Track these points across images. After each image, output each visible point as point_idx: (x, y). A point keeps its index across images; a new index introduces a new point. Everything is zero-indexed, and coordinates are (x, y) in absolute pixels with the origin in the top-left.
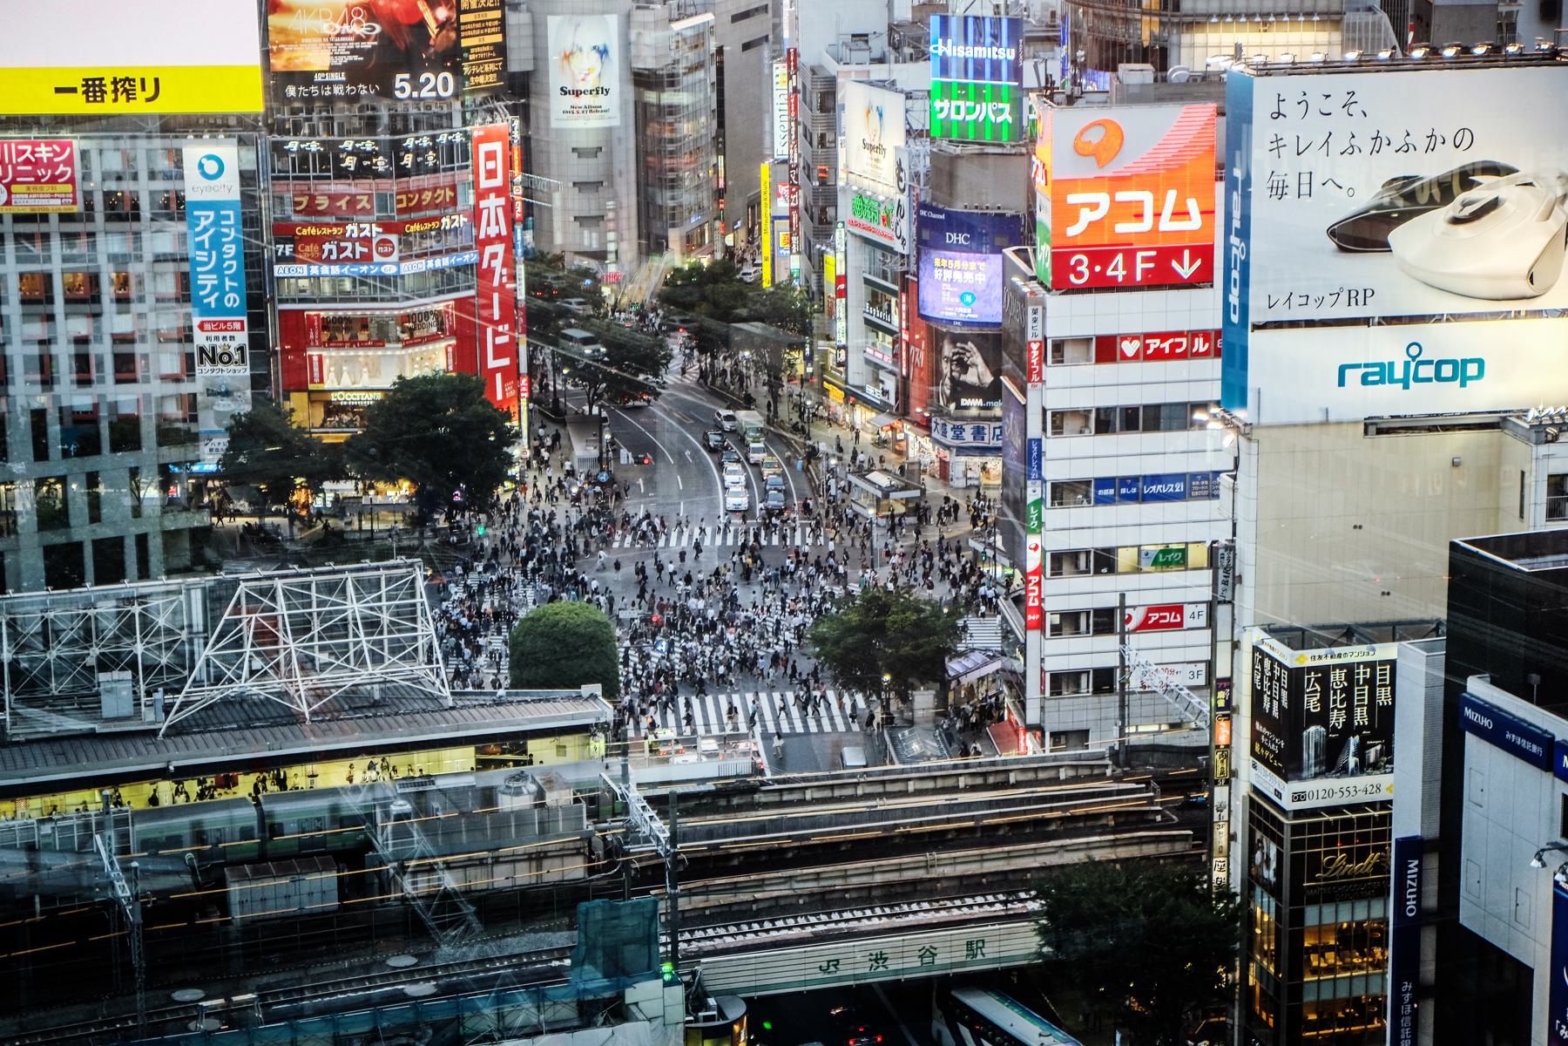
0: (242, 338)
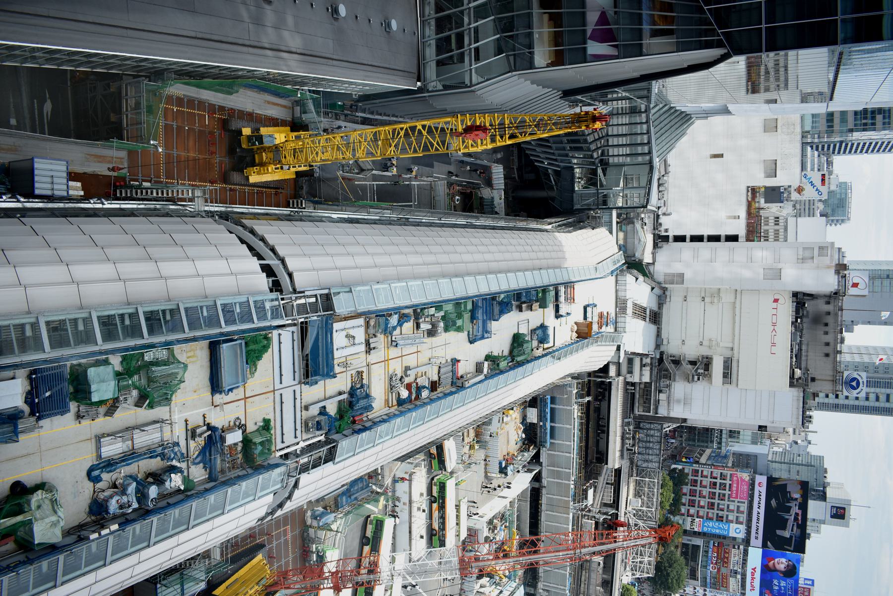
0: (696, 530)
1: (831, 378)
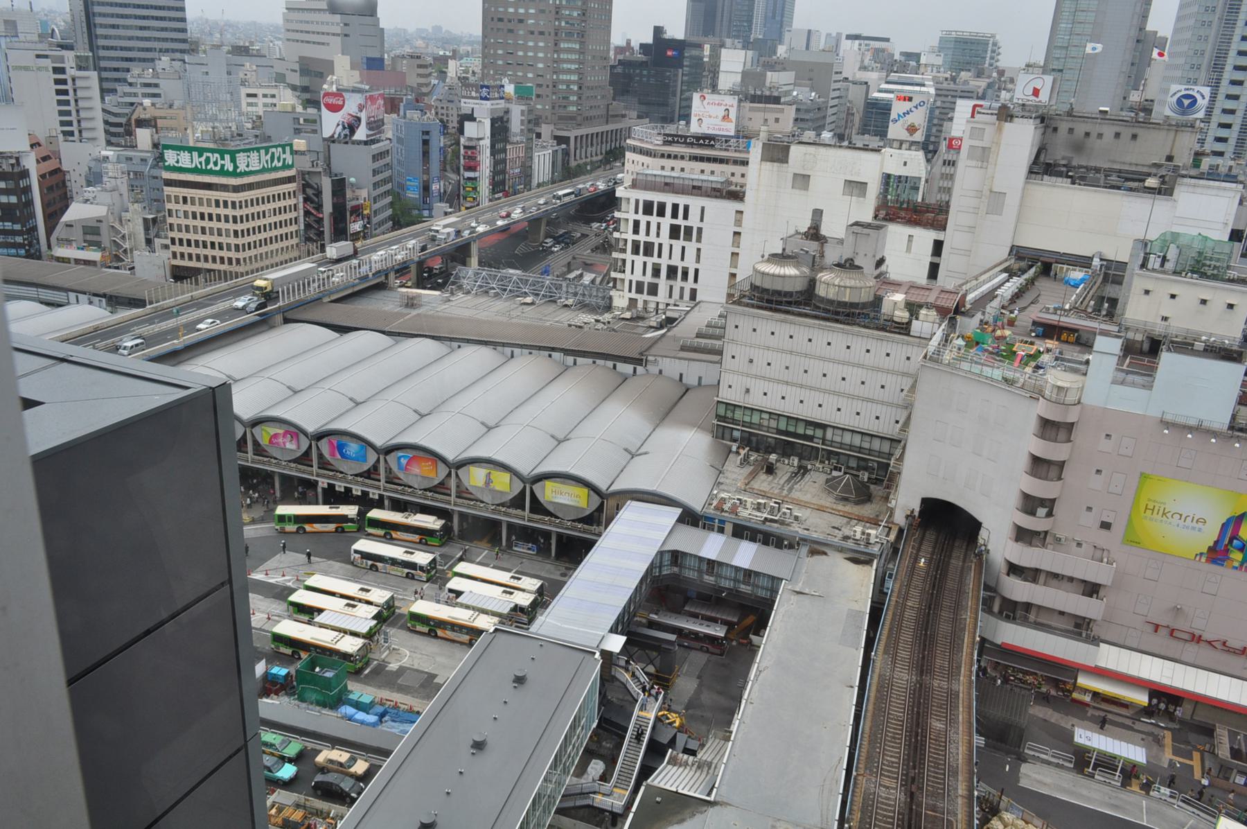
1: (1172, 134)
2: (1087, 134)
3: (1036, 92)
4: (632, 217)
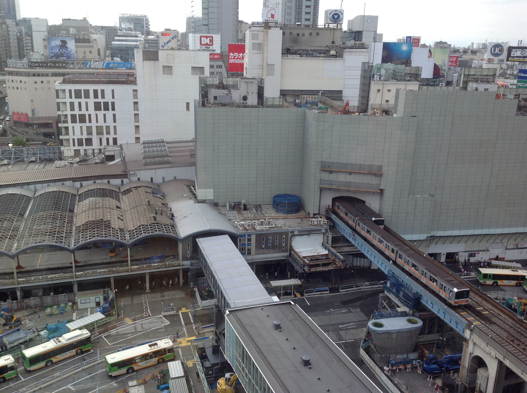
2: (298, 34)
3: (273, 16)
4: (68, 100)
